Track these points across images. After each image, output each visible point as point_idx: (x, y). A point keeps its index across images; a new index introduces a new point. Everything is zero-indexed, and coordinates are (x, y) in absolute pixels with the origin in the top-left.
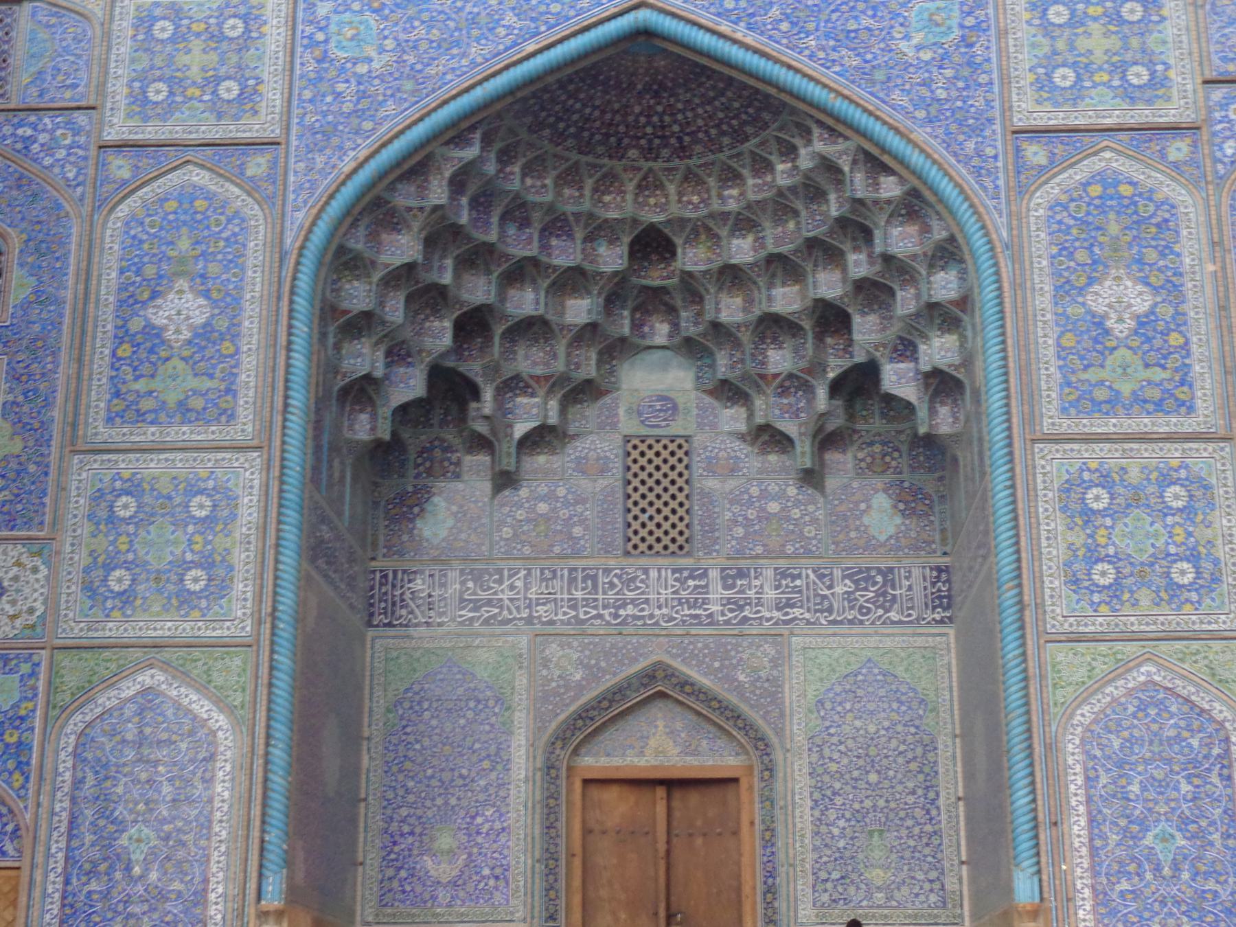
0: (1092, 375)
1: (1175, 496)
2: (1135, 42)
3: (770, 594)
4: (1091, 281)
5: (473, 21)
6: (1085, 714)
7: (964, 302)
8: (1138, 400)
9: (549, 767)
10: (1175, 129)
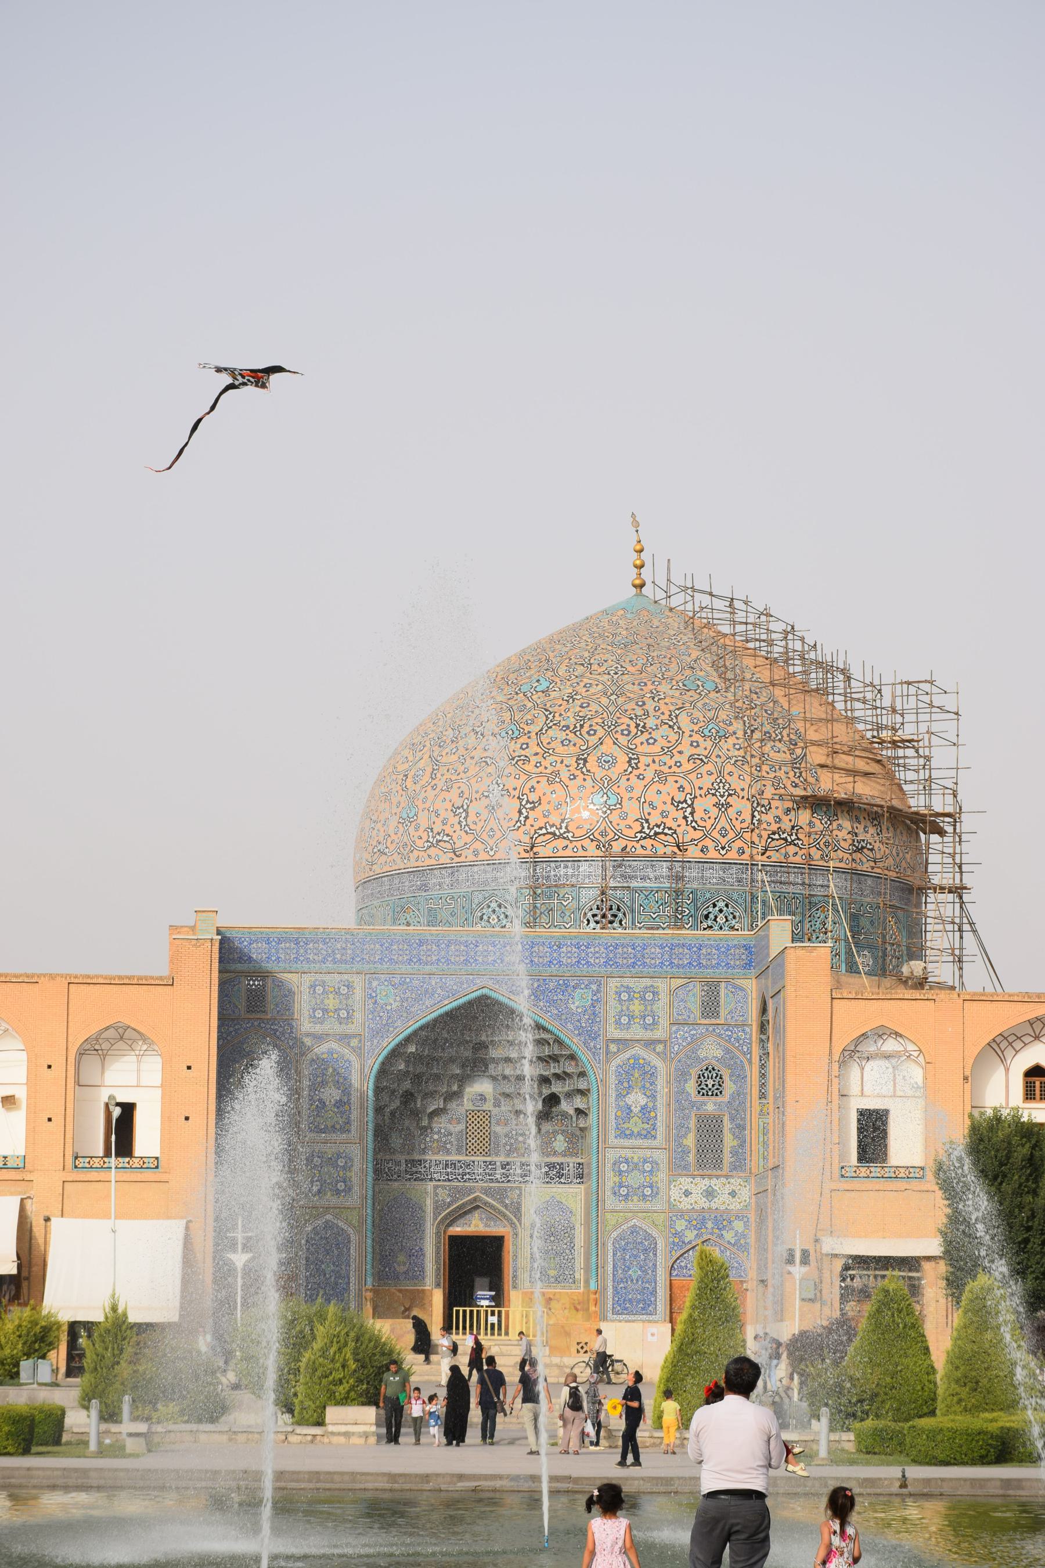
0: (626, 1126)
1: (648, 1167)
2: (649, 1008)
3: (519, 1171)
4: (628, 1093)
5: (427, 991)
6: (615, 1234)
7: (588, 1090)
8: (639, 1134)
9: (438, 1233)
10: (660, 1041)
